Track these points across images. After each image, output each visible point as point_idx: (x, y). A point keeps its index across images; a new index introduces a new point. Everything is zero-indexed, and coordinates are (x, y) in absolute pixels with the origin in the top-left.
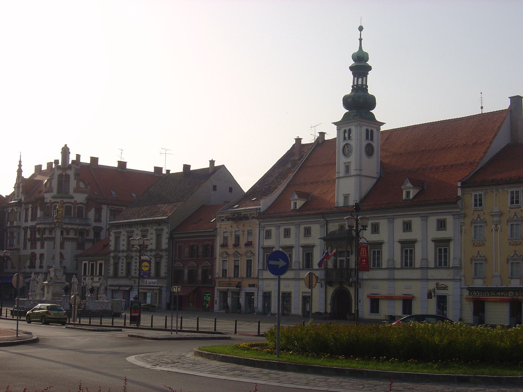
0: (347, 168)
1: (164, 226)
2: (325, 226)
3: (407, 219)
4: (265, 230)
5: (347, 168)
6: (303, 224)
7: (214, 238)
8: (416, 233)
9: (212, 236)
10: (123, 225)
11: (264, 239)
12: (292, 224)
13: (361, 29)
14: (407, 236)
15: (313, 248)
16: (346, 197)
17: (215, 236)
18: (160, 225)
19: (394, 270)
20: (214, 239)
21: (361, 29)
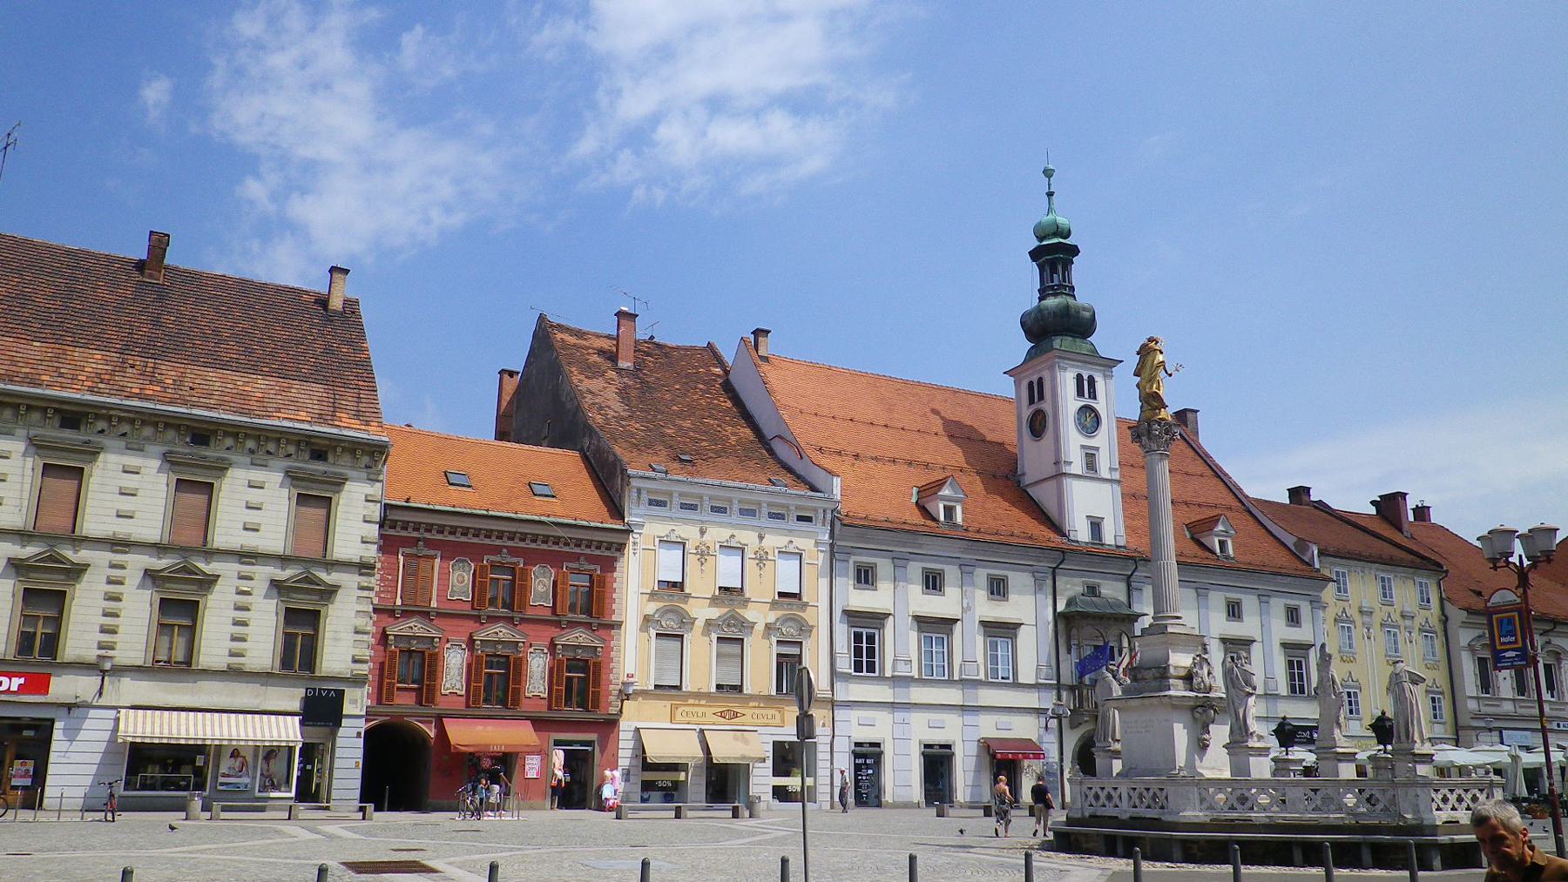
0: (1090, 459)
1: (353, 468)
2: (1049, 582)
3: (1234, 596)
4: (851, 562)
5: (1090, 459)
6: (984, 567)
7: (614, 555)
8: (1247, 627)
9: (609, 547)
10: (16, 407)
11: (851, 587)
12: (950, 559)
13: (1048, 173)
14: (1235, 630)
15: (1015, 629)
16: (1096, 525)
17: (621, 547)
18: (319, 455)
19: (908, 687)
20: (615, 559)
21: (1048, 173)
